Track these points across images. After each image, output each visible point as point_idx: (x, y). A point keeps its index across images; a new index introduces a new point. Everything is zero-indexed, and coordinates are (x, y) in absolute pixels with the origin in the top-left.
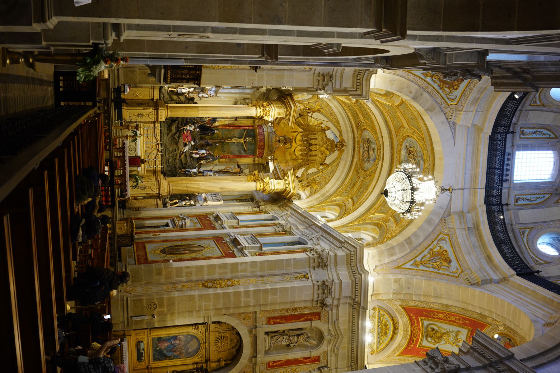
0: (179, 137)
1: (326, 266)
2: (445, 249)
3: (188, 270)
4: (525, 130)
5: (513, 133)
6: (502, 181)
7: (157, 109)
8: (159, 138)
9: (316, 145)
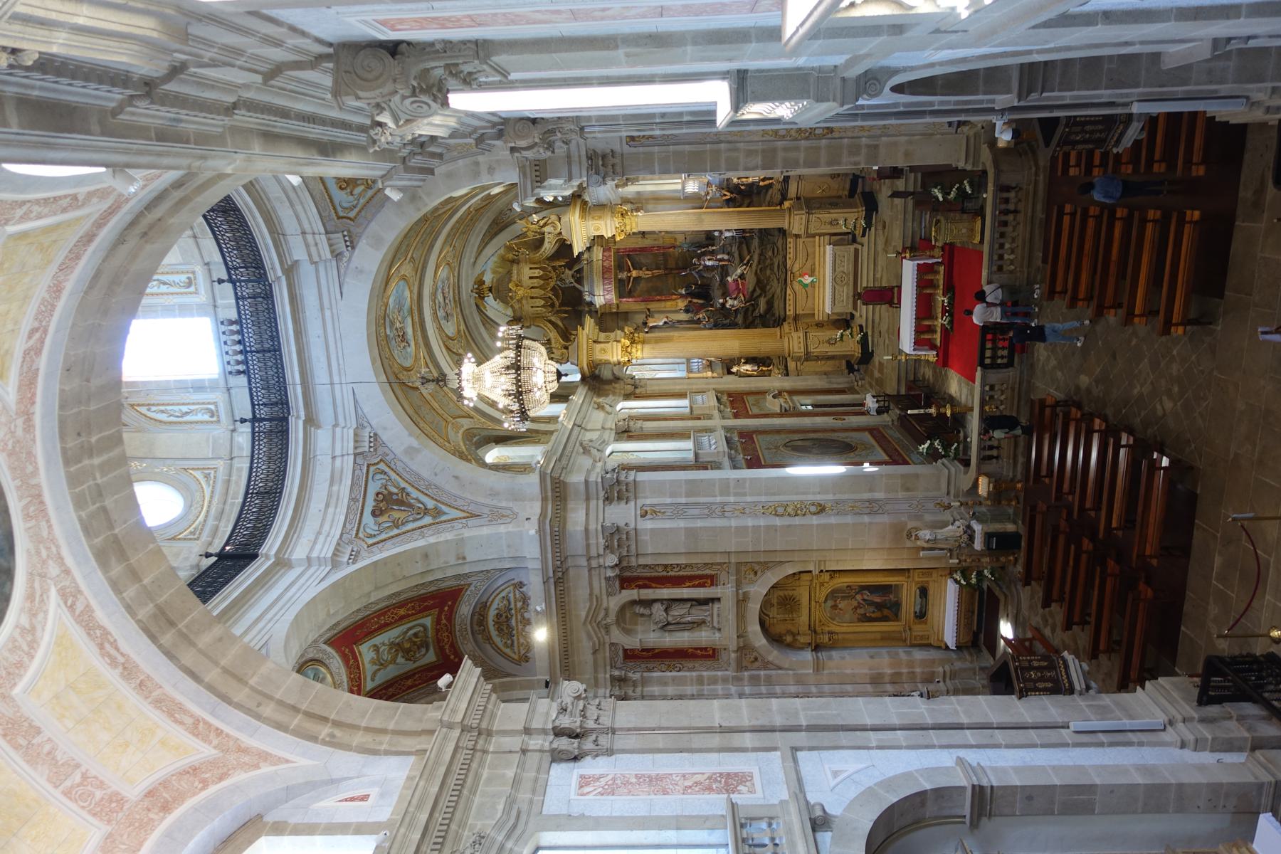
0: (754, 290)
1: (589, 158)
2: (343, 193)
3: (856, 159)
4: (207, 417)
5: (243, 421)
6: (239, 322)
7: (808, 353)
8: (789, 292)
9: (532, 298)
